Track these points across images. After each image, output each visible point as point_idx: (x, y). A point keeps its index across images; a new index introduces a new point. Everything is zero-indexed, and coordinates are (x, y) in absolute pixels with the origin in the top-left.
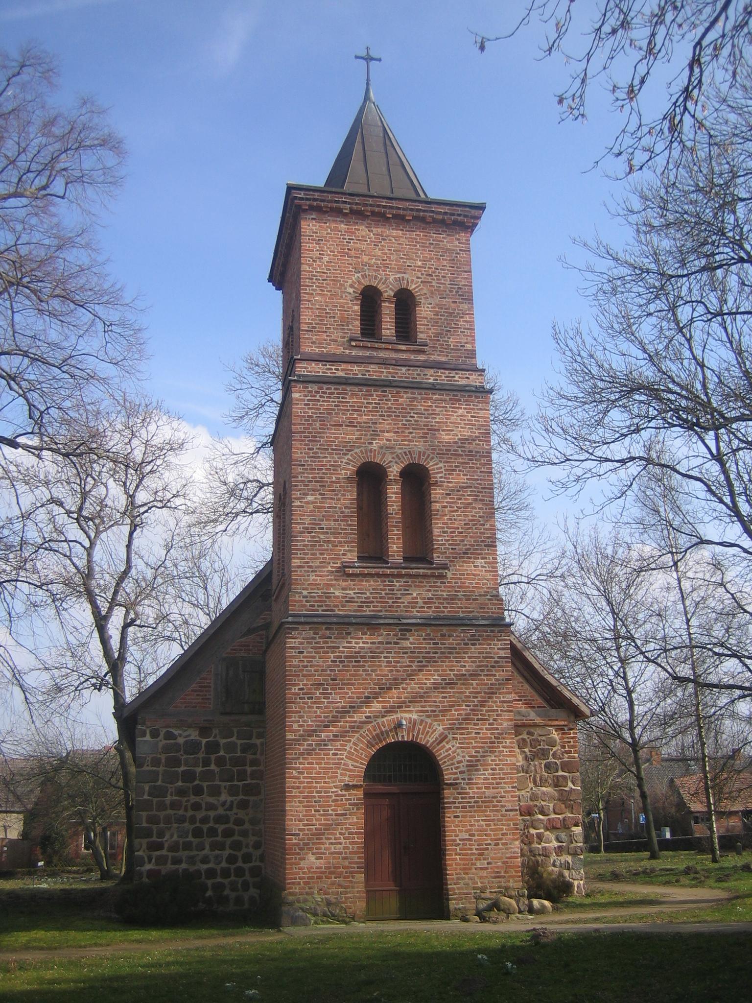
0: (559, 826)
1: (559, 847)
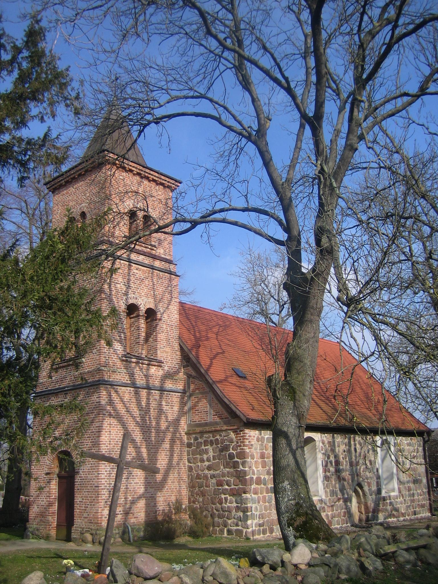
0: (235, 493)
1: (237, 506)
